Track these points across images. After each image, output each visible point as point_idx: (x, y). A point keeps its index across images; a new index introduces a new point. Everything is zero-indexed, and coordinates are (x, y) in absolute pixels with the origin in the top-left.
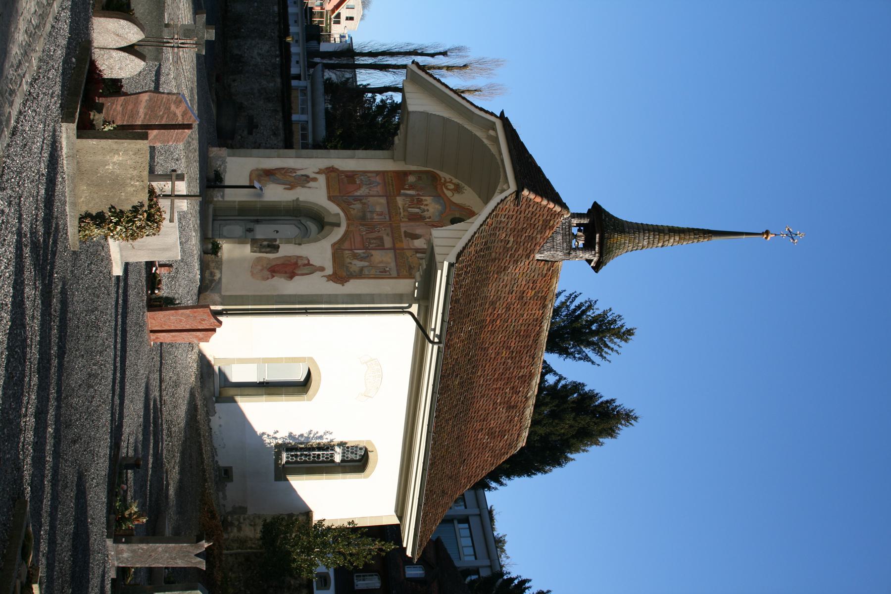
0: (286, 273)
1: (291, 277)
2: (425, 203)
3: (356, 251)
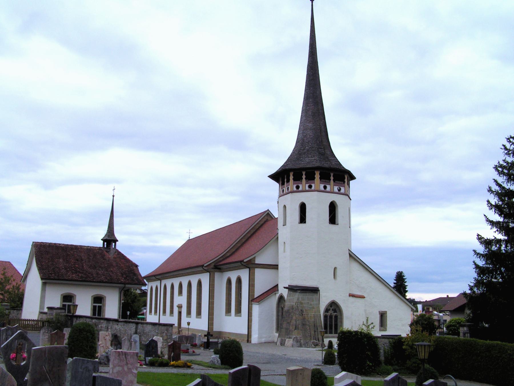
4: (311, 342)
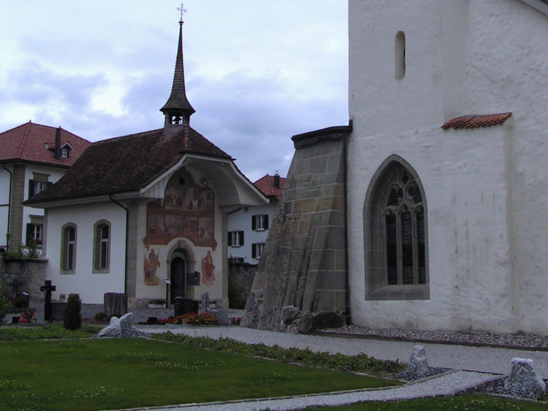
0: (211, 269)
2: (169, 194)
3: (199, 235)
4: (281, 309)
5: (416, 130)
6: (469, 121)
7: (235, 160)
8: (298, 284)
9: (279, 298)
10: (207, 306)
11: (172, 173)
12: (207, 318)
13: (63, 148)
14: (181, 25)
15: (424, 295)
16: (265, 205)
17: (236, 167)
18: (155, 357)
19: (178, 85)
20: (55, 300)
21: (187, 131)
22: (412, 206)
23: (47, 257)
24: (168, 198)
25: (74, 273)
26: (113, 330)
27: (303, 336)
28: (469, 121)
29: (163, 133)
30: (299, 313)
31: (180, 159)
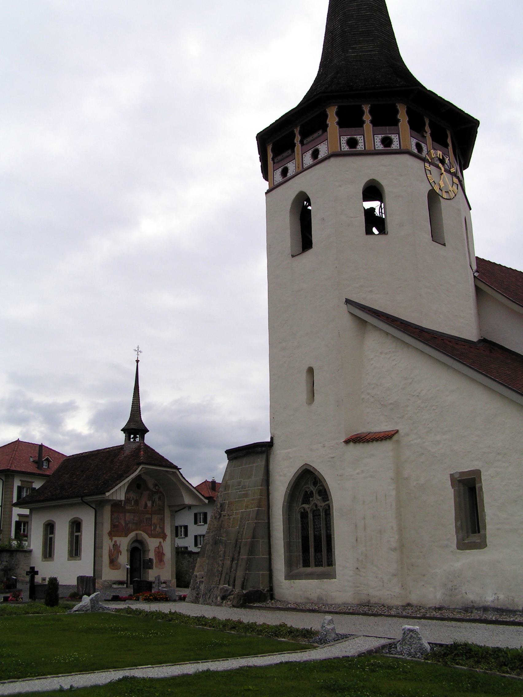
1: (164, 554)
2: (129, 497)
3: (152, 529)
4: (218, 587)
5: (323, 445)
6: (365, 437)
7: (181, 469)
8: (231, 567)
9: (217, 579)
10: (159, 586)
11: (131, 480)
12: (159, 595)
13: (44, 460)
14: (137, 363)
15: (331, 575)
16: (205, 504)
17: (181, 474)
18: (118, 628)
19: (135, 411)
20: (38, 583)
21: (143, 446)
22: (321, 504)
23: (31, 548)
24: (127, 500)
25: (53, 560)
26: (84, 606)
27: (236, 609)
28: (365, 437)
29: (124, 448)
30: (232, 591)
31: (137, 469)
